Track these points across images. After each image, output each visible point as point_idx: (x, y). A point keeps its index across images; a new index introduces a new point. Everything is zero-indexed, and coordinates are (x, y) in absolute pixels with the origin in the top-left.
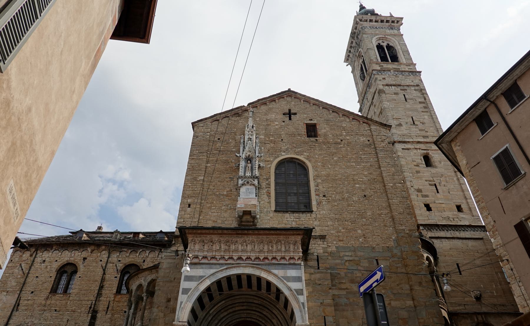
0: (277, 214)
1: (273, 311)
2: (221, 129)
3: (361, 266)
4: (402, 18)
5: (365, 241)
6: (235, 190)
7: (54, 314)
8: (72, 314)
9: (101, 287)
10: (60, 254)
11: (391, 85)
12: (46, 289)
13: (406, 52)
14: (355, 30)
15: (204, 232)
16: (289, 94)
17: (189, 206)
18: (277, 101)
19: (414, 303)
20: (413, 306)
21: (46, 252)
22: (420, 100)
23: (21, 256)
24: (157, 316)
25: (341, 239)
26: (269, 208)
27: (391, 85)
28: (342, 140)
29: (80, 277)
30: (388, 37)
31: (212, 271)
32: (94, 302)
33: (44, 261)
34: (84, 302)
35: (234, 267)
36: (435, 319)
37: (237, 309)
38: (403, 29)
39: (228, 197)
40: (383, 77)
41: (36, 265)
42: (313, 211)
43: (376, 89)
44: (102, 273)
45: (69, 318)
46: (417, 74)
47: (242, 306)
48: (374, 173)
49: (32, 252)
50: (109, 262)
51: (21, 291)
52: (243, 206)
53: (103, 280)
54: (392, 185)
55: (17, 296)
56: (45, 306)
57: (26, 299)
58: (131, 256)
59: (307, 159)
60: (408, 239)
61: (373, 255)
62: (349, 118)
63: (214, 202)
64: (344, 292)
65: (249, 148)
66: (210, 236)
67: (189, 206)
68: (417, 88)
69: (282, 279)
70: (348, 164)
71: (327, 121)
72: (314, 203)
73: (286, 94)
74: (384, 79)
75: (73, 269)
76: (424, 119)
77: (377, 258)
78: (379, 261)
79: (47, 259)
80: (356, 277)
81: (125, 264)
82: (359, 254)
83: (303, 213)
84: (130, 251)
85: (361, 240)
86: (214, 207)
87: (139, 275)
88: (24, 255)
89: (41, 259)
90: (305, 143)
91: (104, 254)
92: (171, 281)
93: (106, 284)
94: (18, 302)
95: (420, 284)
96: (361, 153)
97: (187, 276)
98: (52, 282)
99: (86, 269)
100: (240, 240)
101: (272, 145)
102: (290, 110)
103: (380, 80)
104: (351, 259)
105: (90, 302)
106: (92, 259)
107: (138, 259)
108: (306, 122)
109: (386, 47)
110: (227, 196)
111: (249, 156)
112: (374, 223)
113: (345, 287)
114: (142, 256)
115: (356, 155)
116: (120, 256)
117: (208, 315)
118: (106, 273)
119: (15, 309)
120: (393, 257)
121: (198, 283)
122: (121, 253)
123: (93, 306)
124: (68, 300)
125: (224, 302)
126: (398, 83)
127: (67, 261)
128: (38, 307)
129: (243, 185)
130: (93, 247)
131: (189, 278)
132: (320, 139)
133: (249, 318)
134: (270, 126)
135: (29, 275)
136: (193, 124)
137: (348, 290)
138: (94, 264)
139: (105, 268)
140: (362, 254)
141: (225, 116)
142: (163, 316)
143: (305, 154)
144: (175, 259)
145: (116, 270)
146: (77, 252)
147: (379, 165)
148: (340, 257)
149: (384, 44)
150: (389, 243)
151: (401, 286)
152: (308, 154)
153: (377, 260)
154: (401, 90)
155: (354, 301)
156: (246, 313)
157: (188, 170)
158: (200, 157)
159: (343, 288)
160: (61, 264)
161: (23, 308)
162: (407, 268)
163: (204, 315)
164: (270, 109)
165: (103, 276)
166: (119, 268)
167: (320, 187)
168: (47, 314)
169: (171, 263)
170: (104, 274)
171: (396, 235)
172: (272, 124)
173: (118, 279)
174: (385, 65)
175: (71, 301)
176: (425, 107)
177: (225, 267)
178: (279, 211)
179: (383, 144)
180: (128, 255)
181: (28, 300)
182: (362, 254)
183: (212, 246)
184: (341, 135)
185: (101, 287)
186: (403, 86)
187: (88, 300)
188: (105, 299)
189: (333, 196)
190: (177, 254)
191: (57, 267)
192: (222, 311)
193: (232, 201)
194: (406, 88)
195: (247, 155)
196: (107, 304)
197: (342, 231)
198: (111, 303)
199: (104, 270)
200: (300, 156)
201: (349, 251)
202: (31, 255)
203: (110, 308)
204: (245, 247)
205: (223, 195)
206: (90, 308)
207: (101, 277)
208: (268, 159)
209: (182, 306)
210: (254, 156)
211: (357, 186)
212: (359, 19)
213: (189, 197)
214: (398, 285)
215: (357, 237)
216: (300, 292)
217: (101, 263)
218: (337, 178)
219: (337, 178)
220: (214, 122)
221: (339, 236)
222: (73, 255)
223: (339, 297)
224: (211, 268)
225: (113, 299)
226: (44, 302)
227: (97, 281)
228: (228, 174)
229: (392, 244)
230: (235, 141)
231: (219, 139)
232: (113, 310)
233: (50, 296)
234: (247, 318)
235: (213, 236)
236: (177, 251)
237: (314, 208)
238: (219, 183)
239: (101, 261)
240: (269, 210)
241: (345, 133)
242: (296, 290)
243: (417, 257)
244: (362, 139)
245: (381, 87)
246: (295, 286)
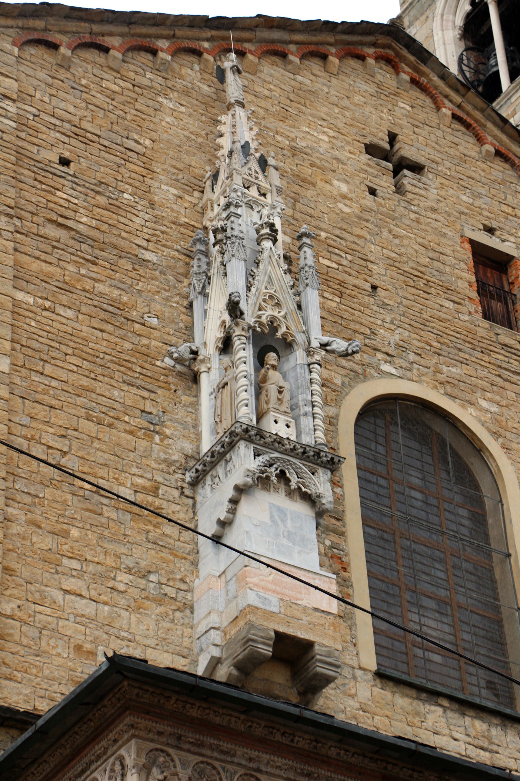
0: (387, 694)
2: (71, 109)
6: (176, 493)
15: (218, 720)
18: (334, 60)
26: (352, 648)
39: (141, 526)
59: (496, 435)
63: (75, 532)
65: (270, 280)
66: (254, 754)
83: (504, 726)
86: (75, 564)
108: (470, 234)
134: (310, 193)
141: (87, 39)
143: (484, 404)
152: (494, 409)
172: (320, 184)
178: (398, 682)
193: (165, 554)
195: (264, 319)
200: (463, 406)
210: (300, 338)
228: (134, 390)
231: (65, 162)
235: (265, 757)
238: (91, 427)
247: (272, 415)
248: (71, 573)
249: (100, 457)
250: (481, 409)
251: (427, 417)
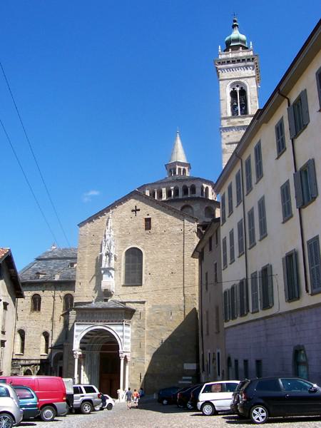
72: (143, 279)
74: (228, 136)
131: (77, 331)
164: (124, 207)
167: (148, 267)
170: (55, 300)
237: (143, 283)
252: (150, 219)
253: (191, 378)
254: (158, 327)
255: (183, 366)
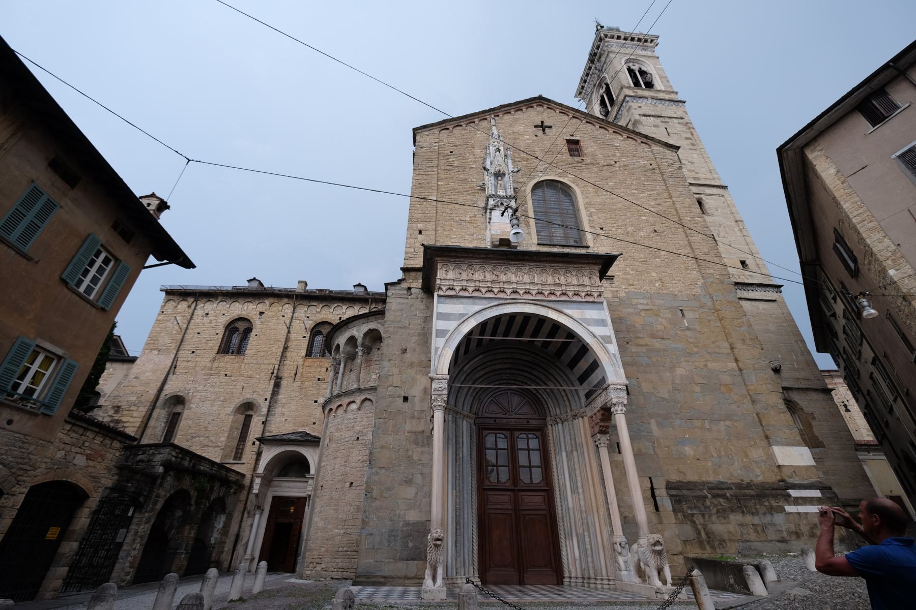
1: (549, 371)
3: (662, 318)
4: (657, 37)
5: (663, 286)
7: (225, 379)
8: (248, 380)
9: (286, 348)
10: (228, 306)
11: (649, 116)
12: (212, 348)
13: (663, 78)
14: (596, 51)
16: (540, 101)
17: (420, 232)
18: (524, 109)
19: (738, 366)
20: (737, 368)
21: (208, 303)
22: (686, 136)
23: (176, 307)
24: (389, 371)
25: (631, 282)
27: (649, 116)
28: (616, 162)
29: (256, 335)
30: (641, 59)
31: (478, 308)
32: (277, 366)
33: (207, 314)
34: (263, 366)
35: (509, 304)
36: (769, 386)
37: (498, 367)
38: (658, 51)
40: (639, 105)
41: (197, 318)
42: (589, 247)
43: (630, 120)
44: (286, 331)
45: (244, 385)
46: (681, 104)
47: (505, 363)
48: (663, 204)
49: (190, 303)
50: (294, 318)
51: (178, 350)
52: (499, 232)
53: (287, 340)
54: (689, 219)
55: (173, 356)
56: (211, 369)
57: (186, 359)
58: (323, 312)
59: (574, 183)
60: (719, 285)
61: (676, 304)
62: (622, 136)
63: (454, 230)
64: (644, 349)
67: (420, 232)
68: (680, 121)
69: (580, 321)
70: (628, 191)
71: (594, 138)
73: (536, 103)
74: (640, 107)
75: (247, 325)
76: (693, 158)
77: (681, 308)
78: (685, 312)
79: (211, 313)
80: (657, 331)
81: (315, 322)
82: (658, 302)
84: (321, 306)
85: (657, 285)
87: (349, 325)
88: (179, 306)
89: (203, 311)
90: (567, 163)
91: (287, 309)
92: (405, 328)
93: (292, 345)
94: (174, 364)
95: (743, 341)
96: (643, 178)
97: (441, 313)
98: (220, 341)
99: (264, 326)
100: (513, 269)
101: (525, 164)
102: (542, 122)
103: (636, 109)
104: (647, 307)
105: (271, 367)
106: (271, 313)
107: (332, 316)
109: (638, 71)
110: (470, 222)
111: (499, 171)
112: (670, 264)
113: (644, 343)
114: (338, 313)
115: (637, 181)
116: (309, 312)
117: (461, 373)
118: (291, 332)
119: (172, 371)
120: (702, 306)
121: (459, 322)
122: (310, 308)
123: (275, 372)
124: (242, 363)
125: (482, 356)
126: (659, 114)
127: (238, 315)
128: (202, 370)
129: (495, 206)
130: (272, 300)
132: (588, 159)
133: (512, 380)
134: (518, 141)
135: (188, 331)
136: (415, 130)
137: (648, 346)
138: (275, 320)
139: (290, 325)
140: (662, 302)
141: (456, 124)
142: (398, 373)
144: (408, 298)
145: (303, 328)
146: (251, 304)
147: (670, 194)
148: (632, 304)
149: (636, 68)
150: (695, 291)
151: (717, 344)
153: (681, 310)
154: (662, 122)
155: (657, 360)
156: (509, 374)
157: (414, 187)
158: (428, 173)
159: (641, 343)
160: (230, 319)
161: (181, 371)
162: (722, 322)
163: (457, 372)
164: (516, 120)
165: (287, 335)
166: (308, 326)
167: (595, 218)
168: (214, 379)
169: (403, 303)
170: (289, 332)
171: (702, 281)
172: (521, 138)
173: (307, 339)
174: (640, 92)
175: (246, 364)
176: (693, 144)
177: (496, 303)
179: (670, 169)
180: (318, 310)
181: (188, 361)
182: (662, 302)
183: (473, 274)
184: (614, 156)
185: (286, 348)
186: (664, 117)
187: (269, 364)
188: (291, 363)
189: (614, 229)
190: (409, 293)
191: (225, 322)
192: (479, 369)
193: (478, 229)
194: (667, 120)
196: (295, 369)
197: (631, 272)
198: (300, 368)
199: (289, 328)
201: (643, 299)
202: (189, 307)
203: (298, 374)
204: (521, 277)
205: (465, 221)
206: (273, 373)
207: (285, 336)
208: (521, 180)
209: (439, 353)
210: (507, 172)
211: (644, 218)
212: (604, 34)
213: (419, 221)
214: (713, 342)
215: (652, 281)
216: (607, 339)
217: (283, 319)
218: (615, 207)
219: (615, 207)
220: (443, 131)
221: (627, 279)
222: (245, 308)
223: (637, 356)
224: (474, 304)
225: (302, 363)
226: (209, 365)
227: (280, 341)
229: (698, 291)
230: (474, 155)
231: (451, 152)
232: (302, 376)
233: (218, 357)
234: (509, 380)
236: (409, 289)
239: (284, 316)
240: (529, 242)
241: (619, 154)
242: (603, 337)
243: (734, 309)
244: (642, 162)
245: (638, 117)
246: (599, 331)
247: (498, 191)
248: (453, 238)
249: (461, 212)
250: (569, 178)
251: (555, 183)
252: (577, 142)
253: (817, 493)
254: (657, 344)
255: (771, 457)
